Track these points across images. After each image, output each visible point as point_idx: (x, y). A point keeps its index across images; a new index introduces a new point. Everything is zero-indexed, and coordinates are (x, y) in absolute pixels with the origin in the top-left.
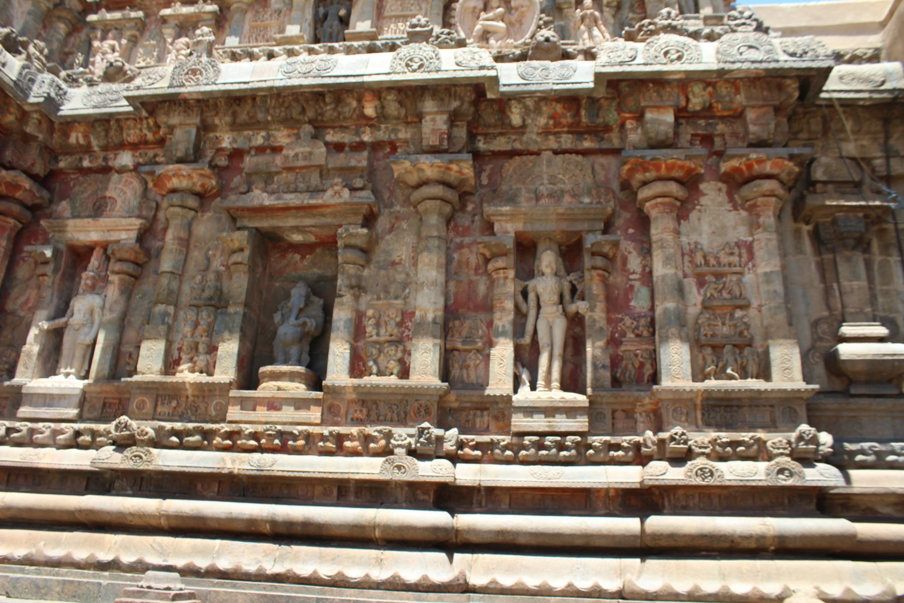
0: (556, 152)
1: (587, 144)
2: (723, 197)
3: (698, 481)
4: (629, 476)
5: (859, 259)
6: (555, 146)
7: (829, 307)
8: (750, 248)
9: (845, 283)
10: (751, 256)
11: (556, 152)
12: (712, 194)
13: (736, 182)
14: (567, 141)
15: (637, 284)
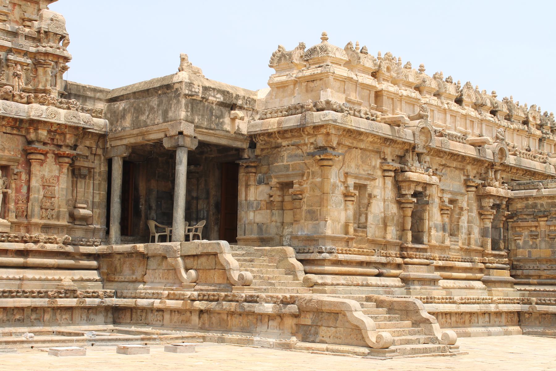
0: (4, 133)
1: (15, 132)
2: (53, 160)
3: (41, 249)
4: (21, 246)
5: (83, 181)
6: (5, 131)
7: (73, 196)
8: (58, 177)
9: (78, 189)
10: (58, 180)
11: (4, 133)
12: (50, 158)
13: (58, 156)
14: (9, 130)
15: (24, 184)
